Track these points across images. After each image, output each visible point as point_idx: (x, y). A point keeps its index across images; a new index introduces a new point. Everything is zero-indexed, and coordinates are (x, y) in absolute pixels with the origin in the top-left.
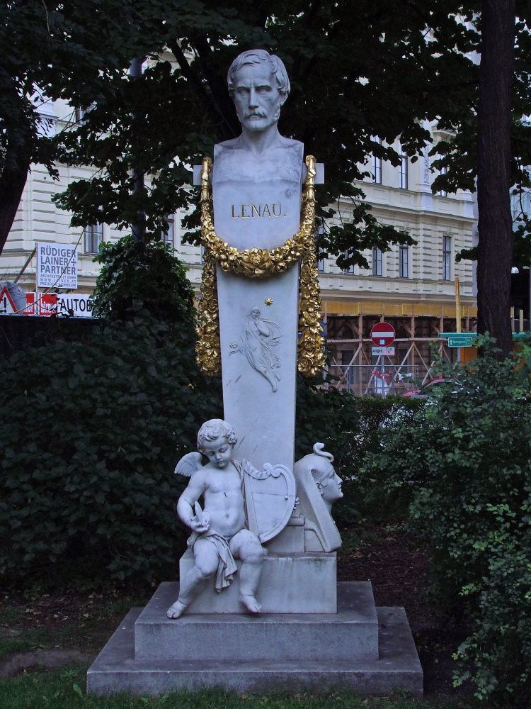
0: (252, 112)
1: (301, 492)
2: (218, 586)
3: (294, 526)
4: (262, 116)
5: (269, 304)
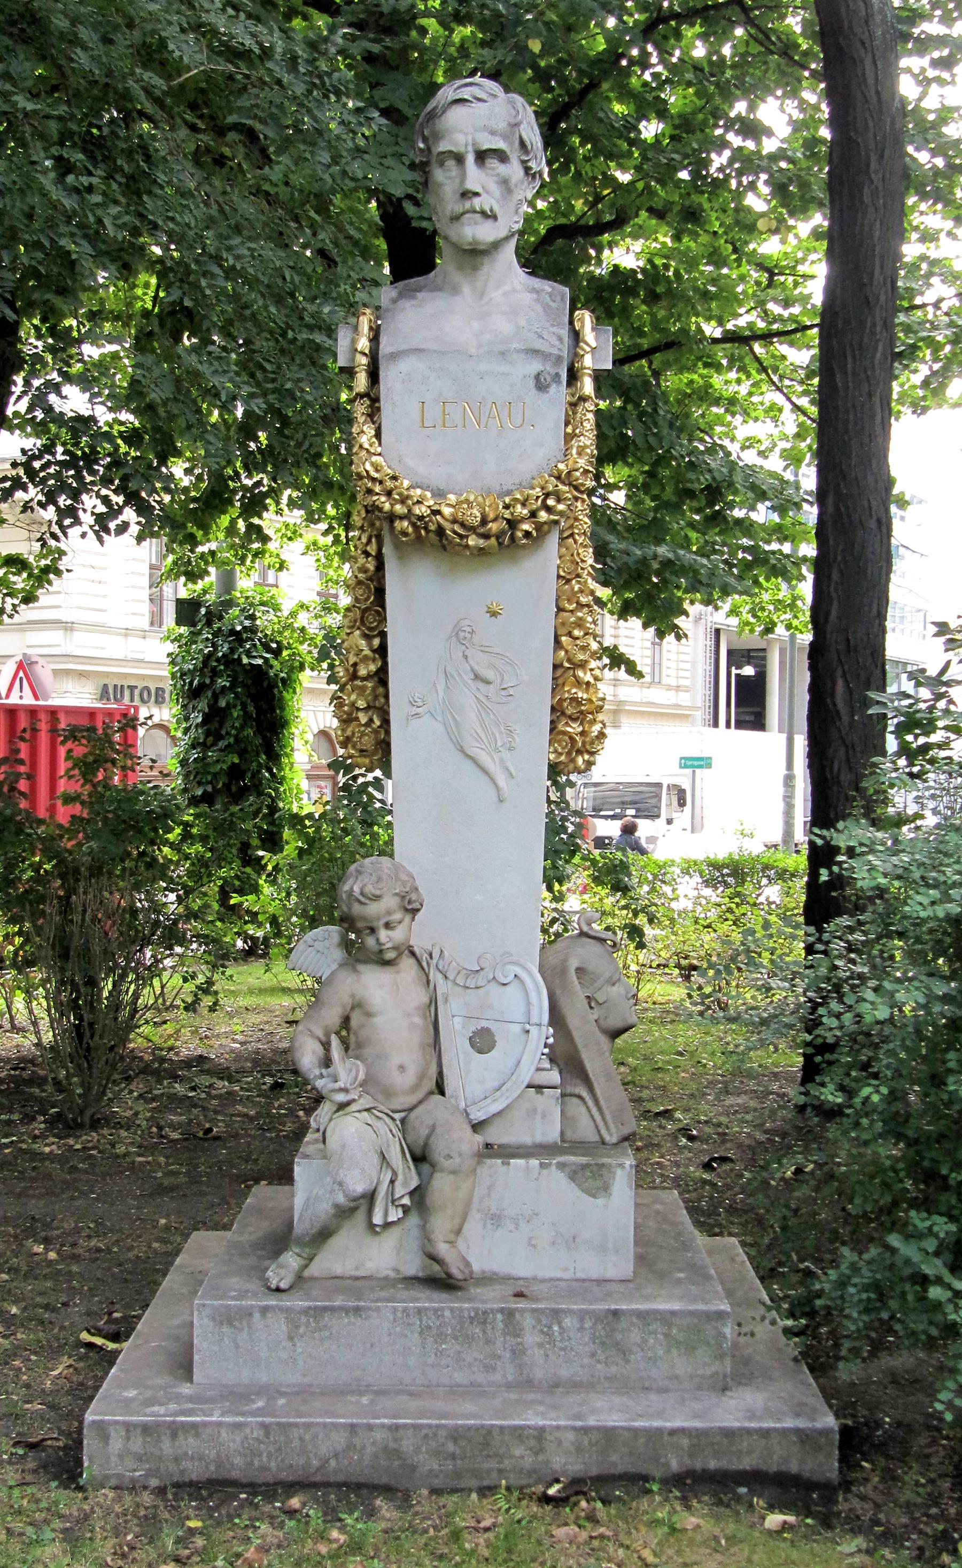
0: (468, 205)
1: (556, 1018)
2: (377, 1219)
4: (491, 216)
5: (494, 614)
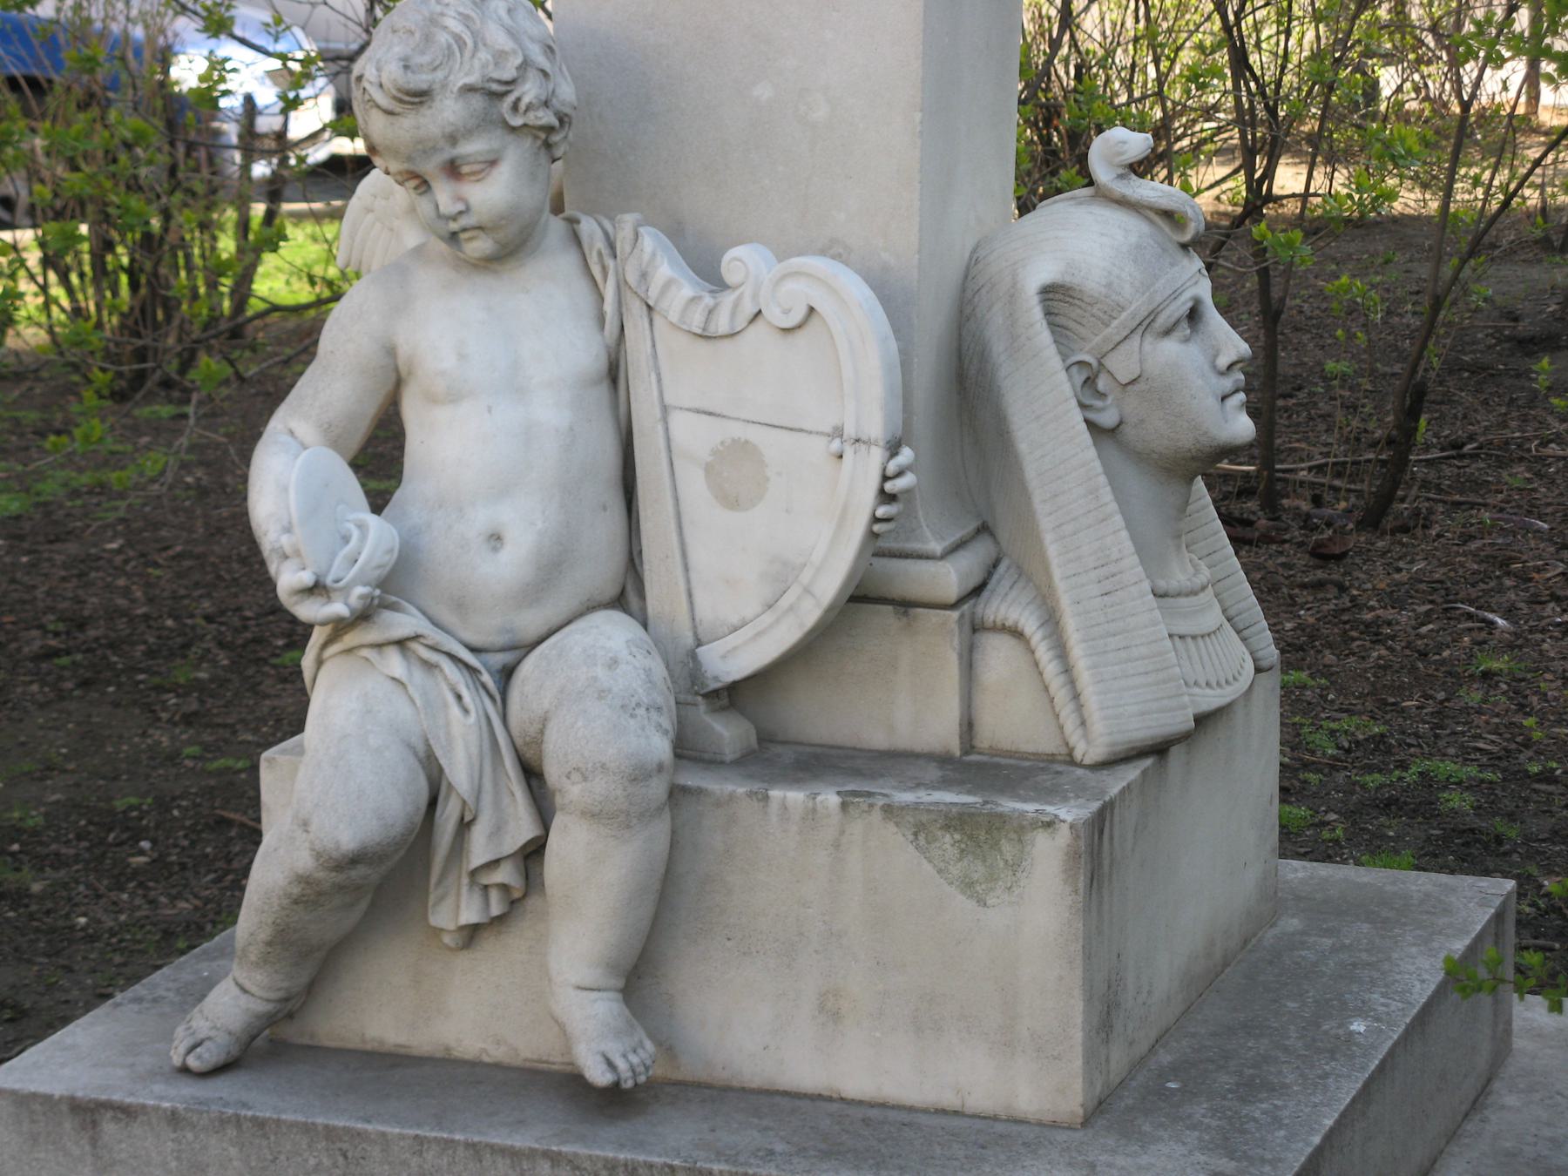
3: (905, 605)
